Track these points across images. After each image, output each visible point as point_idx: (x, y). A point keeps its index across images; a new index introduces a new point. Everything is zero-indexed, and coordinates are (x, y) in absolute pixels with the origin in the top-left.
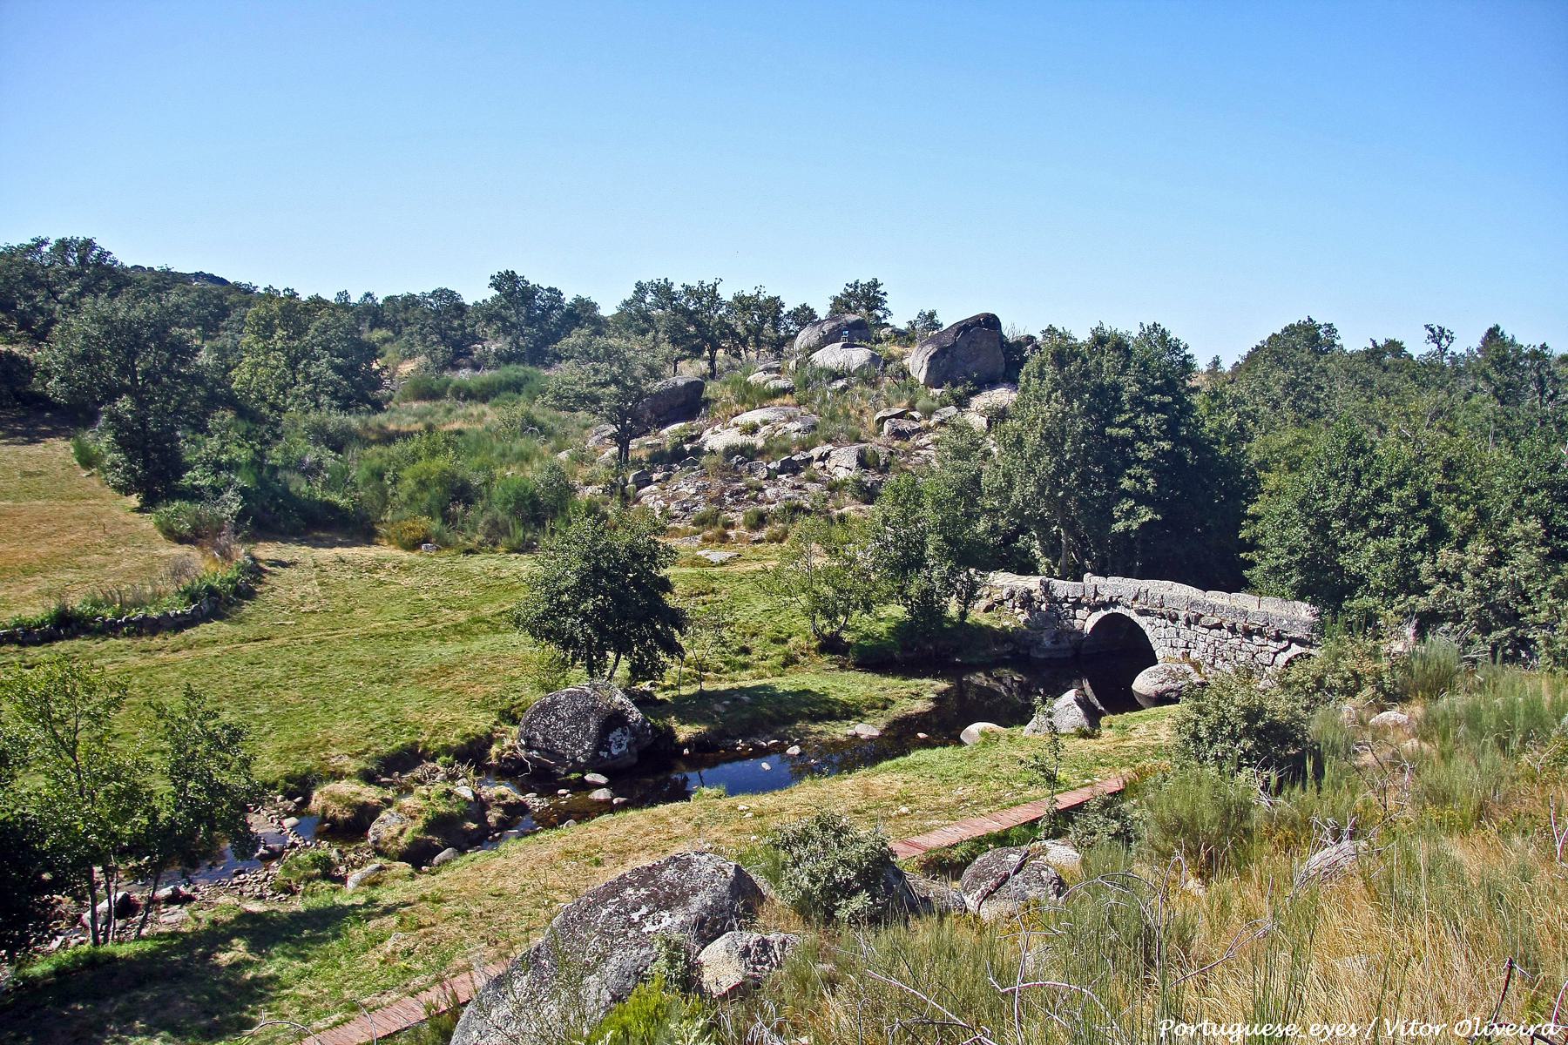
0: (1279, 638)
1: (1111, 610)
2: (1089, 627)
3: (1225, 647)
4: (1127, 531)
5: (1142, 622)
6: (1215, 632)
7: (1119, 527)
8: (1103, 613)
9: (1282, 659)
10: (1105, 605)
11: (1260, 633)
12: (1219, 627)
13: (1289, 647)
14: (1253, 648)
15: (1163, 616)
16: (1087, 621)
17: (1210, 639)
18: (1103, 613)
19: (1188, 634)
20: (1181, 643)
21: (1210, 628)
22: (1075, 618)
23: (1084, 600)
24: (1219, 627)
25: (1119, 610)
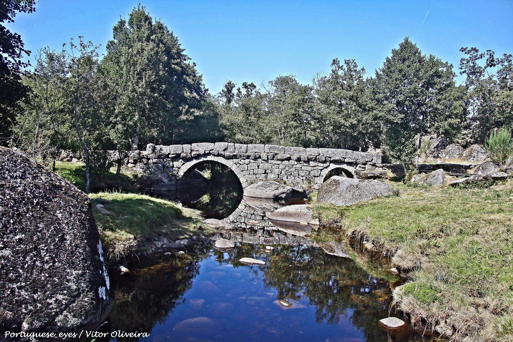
0: (325, 162)
1: (202, 159)
2: (181, 173)
6: (286, 162)
7: (183, 117)
8: (195, 162)
9: (325, 172)
10: (198, 157)
11: (315, 160)
12: (289, 159)
13: (329, 165)
14: (309, 169)
15: (248, 157)
16: (182, 169)
17: (281, 167)
18: (195, 162)
19: (266, 165)
20: (261, 171)
21: (282, 160)
22: (173, 167)
23: (183, 155)
24: (289, 159)
25: (210, 158)
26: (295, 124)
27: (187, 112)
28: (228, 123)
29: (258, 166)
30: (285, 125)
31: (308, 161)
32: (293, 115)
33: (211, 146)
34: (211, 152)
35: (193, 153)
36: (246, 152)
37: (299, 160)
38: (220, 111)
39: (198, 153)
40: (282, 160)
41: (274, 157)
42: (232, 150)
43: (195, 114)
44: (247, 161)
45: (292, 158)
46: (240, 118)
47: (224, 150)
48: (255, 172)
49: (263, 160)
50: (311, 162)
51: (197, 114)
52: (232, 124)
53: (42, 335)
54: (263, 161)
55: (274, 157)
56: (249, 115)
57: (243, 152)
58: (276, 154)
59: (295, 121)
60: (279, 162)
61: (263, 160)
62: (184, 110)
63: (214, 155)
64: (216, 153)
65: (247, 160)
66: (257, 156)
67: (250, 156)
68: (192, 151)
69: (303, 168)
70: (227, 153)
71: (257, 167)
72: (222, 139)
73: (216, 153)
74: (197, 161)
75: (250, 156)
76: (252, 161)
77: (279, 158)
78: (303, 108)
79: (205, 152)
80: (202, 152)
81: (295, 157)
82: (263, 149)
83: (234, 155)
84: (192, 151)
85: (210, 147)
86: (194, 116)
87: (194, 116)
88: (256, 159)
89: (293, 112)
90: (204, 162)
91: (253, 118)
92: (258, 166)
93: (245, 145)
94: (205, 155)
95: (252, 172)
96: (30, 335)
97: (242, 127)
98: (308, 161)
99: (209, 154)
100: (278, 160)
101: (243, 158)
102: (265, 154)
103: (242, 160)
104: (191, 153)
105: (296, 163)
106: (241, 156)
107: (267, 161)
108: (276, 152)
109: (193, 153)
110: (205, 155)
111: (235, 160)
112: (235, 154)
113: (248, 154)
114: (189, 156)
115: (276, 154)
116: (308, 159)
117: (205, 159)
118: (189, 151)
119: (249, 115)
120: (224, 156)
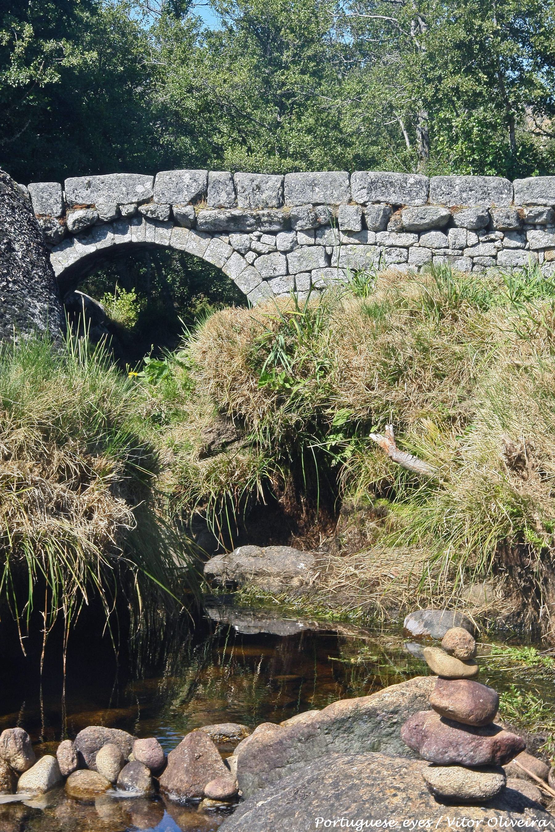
1: (111, 239)
3: (463, 263)
4: (33, 84)
5: (212, 251)
6: (434, 237)
7: (16, 76)
10: (90, 230)
12: (446, 225)
15: (288, 225)
17: (418, 255)
18: (80, 250)
19: (358, 253)
21: (419, 231)
24: (446, 225)
25: (136, 234)
26: (466, 83)
27: (33, 51)
28: (191, 104)
29: (328, 257)
30: (429, 92)
31: (520, 228)
32: (459, 46)
33: (141, 185)
34: (143, 209)
35: (72, 217)
36: (280, 205)
37: (484, 226)
38: (156, 50)
39: (90, 214)
40: (419, 231)
41: (386, 219)
42: (223, 198)
43: (65, 62)
44: (284, 239)
45: (458, 218)
46: (236, 79)
47: (194, 201)
48: (319, 278)
49: (349, 233)
50: (531, 234)
51: (75, 61)
52: (206, 107)
53: (376, 824)
54: (345, 239)
55: (386, 219)
56: (279, 65)
57: (266, 206)
58: (396, 207)
59: (469, 71)
60: (408, 238)
61: (349, 233)
62: (20, 47)
63: (156, 222)
64: (163, 213)
65: (282, 235)
66: (322, 219)
67: (297, 219)
68: (67, 206)
69: (502, 256)
70: (205, 213)
71: (322, 262)
72: (173, 161)
73: (163, 213)
74: (91, 248)
75: (297, 219)
76: (302, 238)
77: (406, 220)
78: (500, 17)
79: (118, 212)
80: (106, 212)
81: (467, 216)
82: (345, 192)
83: (234, 219)
84: (67, 206)
85: (140, 189)
86: (61, 70)
87: (61, 70)
88: (317, 229)
89: (462, 34)
90: (115, 248)
91: (293, 77)
92: (328, 257)
93: (275, 180)
94: (119, 222)
95: (303, 281)
96: (356, 824)
97: (248, 117)
98: (520, 228)
99: (136, 217)
100: (403, 230)
101: (267, 228)
102: (352, 209)
103: (266, 238)
104: (63, 216)
105: (473, 238)
106: (259, 222)
107: (360, 235)
108: (394, 199)
109: (72, 217)
110: (119, 222)
111: (237, 239)
112: (236, 212)
113: (289, 210)
114: (57, 227)
115: (396, 207)
116: (520, 218)
117: (121, 239)
118: (57, 209)
119: (279, 65)
120: (193, 226)
